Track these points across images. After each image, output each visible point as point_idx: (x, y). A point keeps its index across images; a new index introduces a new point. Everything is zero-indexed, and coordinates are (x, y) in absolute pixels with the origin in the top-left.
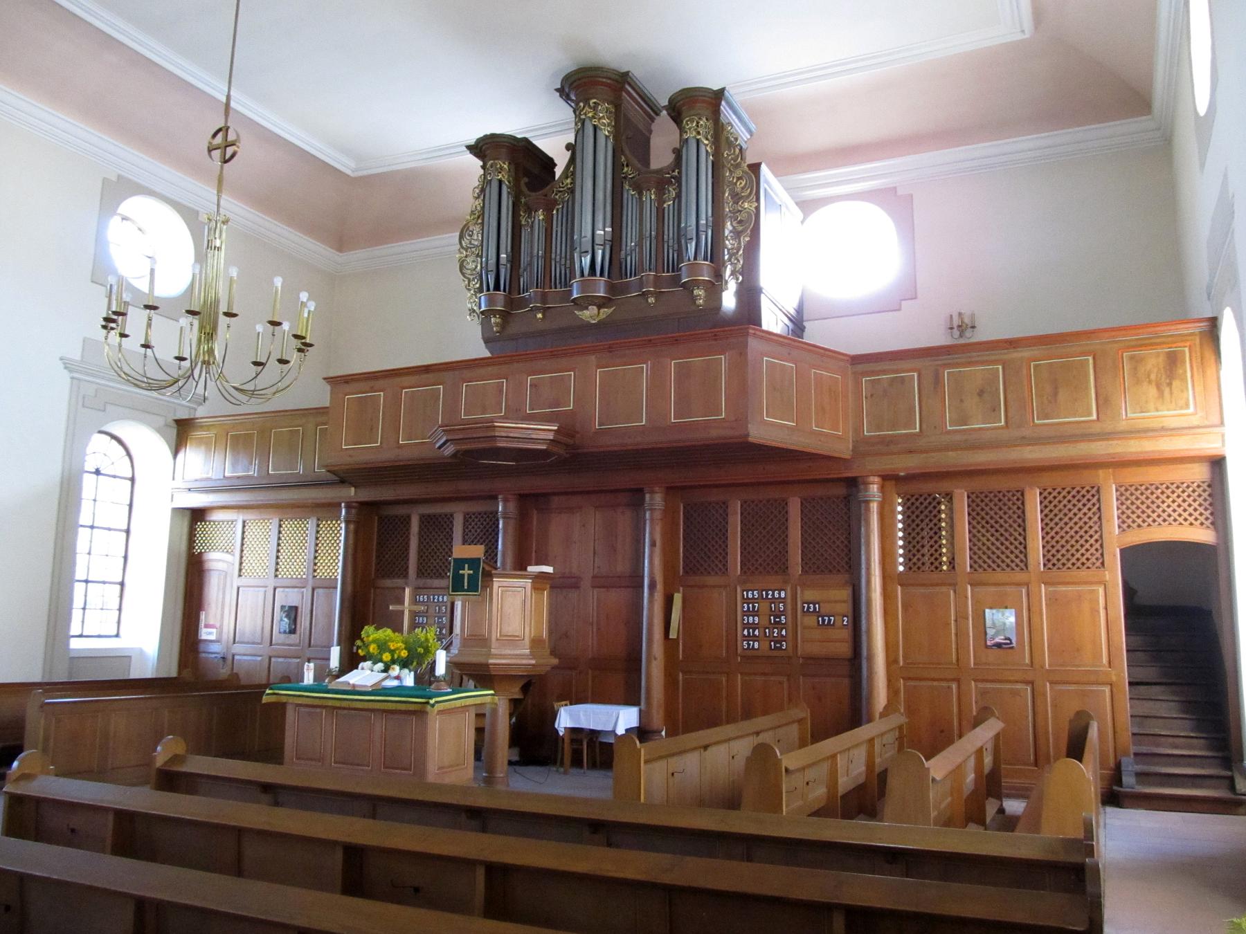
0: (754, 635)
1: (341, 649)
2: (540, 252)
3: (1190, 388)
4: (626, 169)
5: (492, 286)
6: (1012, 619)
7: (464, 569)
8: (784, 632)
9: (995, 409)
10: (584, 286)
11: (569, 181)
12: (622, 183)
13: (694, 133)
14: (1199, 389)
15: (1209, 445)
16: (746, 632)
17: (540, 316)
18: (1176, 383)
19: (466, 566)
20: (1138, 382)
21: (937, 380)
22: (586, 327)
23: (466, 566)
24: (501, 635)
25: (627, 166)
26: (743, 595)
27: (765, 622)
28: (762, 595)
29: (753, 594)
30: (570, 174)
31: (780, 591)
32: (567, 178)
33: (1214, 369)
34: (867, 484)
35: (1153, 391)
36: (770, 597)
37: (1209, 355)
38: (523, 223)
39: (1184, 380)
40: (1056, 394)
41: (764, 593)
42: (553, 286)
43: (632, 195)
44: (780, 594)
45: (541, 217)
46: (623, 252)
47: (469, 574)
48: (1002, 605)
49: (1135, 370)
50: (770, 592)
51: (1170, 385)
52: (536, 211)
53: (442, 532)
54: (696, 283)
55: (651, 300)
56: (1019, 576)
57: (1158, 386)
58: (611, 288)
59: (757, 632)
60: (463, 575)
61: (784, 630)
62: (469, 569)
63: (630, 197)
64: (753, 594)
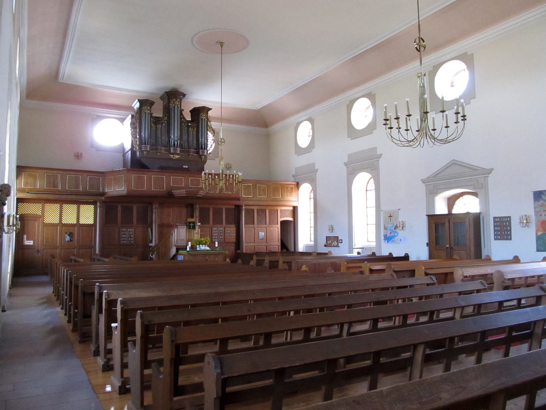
3: (294, 194)
4: (183, 120)
5: (147, 143)
6: (264, 234)
8: (222, 237)
9: (265, 194)
10: (175, 150)
11: (166, 118)
12: (181, 123)
13: (204, 118)
14: (295, 195)
15: (295, 204)
17: (159, 154)
18: (292, 193)
20: (287, 191)
21: (256, 187)
22: (172, 159)
25: (183, 119)
32: (166, 117)
33: (297, 191)
34: (242, 206)
35: (289, 194)
37: (297, 188)
38: (152, 126)
39: (293, 192)
40: (275, 192)
45: (160, 127)
46: (182, 142)
48: (262, 231)
49: (286, 189)
51: (291, 193)
52: (159, 125)
54: (204, 155)
55: (190, 156)
56: (265, 226)
57: (290, 193)
58: (180, 151)
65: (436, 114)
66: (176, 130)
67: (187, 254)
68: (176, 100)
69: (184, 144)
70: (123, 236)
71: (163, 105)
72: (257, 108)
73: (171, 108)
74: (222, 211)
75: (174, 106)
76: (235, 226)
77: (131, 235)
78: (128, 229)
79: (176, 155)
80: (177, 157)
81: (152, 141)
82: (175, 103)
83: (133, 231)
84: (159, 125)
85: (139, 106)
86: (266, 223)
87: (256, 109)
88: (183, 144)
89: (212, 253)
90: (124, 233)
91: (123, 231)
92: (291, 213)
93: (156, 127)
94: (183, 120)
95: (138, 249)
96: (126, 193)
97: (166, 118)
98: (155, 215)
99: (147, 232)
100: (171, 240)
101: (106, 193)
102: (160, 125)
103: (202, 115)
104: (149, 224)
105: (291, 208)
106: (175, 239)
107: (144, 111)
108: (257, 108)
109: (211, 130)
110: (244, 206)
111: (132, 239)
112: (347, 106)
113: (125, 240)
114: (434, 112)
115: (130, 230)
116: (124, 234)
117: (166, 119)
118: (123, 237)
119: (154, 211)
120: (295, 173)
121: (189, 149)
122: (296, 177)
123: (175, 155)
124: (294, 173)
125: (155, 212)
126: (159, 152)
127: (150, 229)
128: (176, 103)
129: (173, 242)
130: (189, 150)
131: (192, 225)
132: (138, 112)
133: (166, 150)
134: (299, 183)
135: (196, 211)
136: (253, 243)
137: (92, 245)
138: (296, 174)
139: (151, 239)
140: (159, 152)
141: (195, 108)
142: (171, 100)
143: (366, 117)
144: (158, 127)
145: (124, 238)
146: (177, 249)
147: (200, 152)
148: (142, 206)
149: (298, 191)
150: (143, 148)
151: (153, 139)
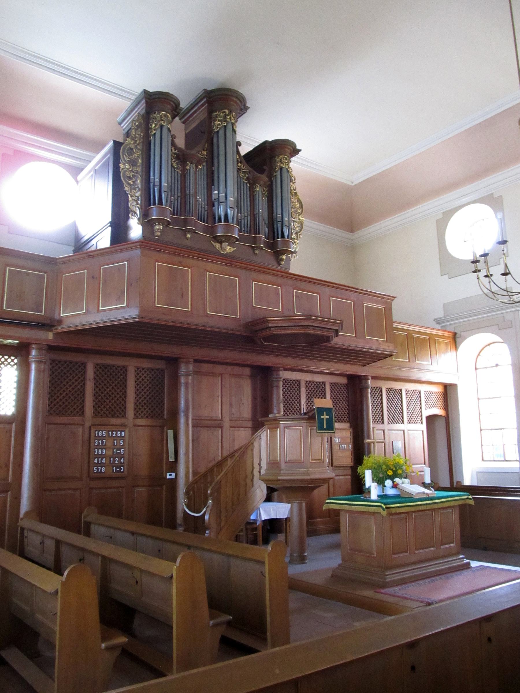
0: (102, 463)
1: (372, 473)
2: (191, 191)
7: (323, 415)
16: (96, 461)
19: (325, 413)
23: (325, 413)
24: (312, 460)
26: (95, 434)
27: (110, 453)
28: (109, 434)
29: (102, 433)
30: (205, 149)
31: (121, 432)
36: (114, 435)
41: (110, 432)
42: (176, 214)
43: (243, 182)
44: (121, 434)
47: (326, 419)
50: (114, 432)
53: (121, 380)
59: (104, 461)
60: (323, 419)
61: (123, 459)
62: (327, 415)
63: (242, 183)
64: (102, 433)
65: (450, 278)
66: (230, 182)
67: (384, 513)
68: (231, 112)
69: (243, 221)
70: (100, 451)
71: (186, 135)
72: (352, 183)
73: (218, 132)
74: (325, 389)
75: (225, 127)
76: (351, 427)
77: (120, 450)
78: (117, 432)
79: (228, 245)
80: (229, 249)
81: (174, 202)
82: (228, 120)
83: (127, 438)
84: (191, 163)
85: (144, 111)
86: (403, 421)
87: (350, 183)
88: (241, 222)
89: (421, 508)
90: (102, 442)
91: (98, 438)
92: (438, 400)
93: (184, 170)
94: (240, 166)
95: (137, 489)
96: (139, 317)
97: (205, 153)
98: (187, 393)
99: (163, 440)
100: (249, 463)
101: (60, 322)
102: (194, 165)
103: (281, 160)
104: (165, 417)
105: (439, 389)
106: (260, 460)
107: (159, 121)
108: (352, 183)
109: (296, 201)
110: (370, 378)
111: (122, 460)
112: (437, 221)
113: (102, 465)
114: (447, 275)
115: (119, 435)
116: (103, 447)
117: (204, 154)
118: (98, 456)
119: (183, 380)
120: (442, 315)
121: (255, 233)
122: (443, 323)
123: (225, 244)
124: (440, 314)
125: (187, 384)
126: (190, 231)
127: (170, 433)
128: (230, 119)
129: (256, 472)
130: (255, 238)
131: (325, 417)
132: (140, 124)
133: (206, 230)
134: (457, 336)
135: (278, 387)
136: (421, 464)
137: (7, 478)
138: (445, 316)
139: (172, 459)
140: (190, 231)
141: (266, 142)
142: (215, 114)
143: (465, 242)
144: (188, 168)
145: (102, 456)
146: (268, 488)
147: (279, 243)
148: (157, 370)
149: (456, 352)
150: (154, 213)
151: (176, 196)
